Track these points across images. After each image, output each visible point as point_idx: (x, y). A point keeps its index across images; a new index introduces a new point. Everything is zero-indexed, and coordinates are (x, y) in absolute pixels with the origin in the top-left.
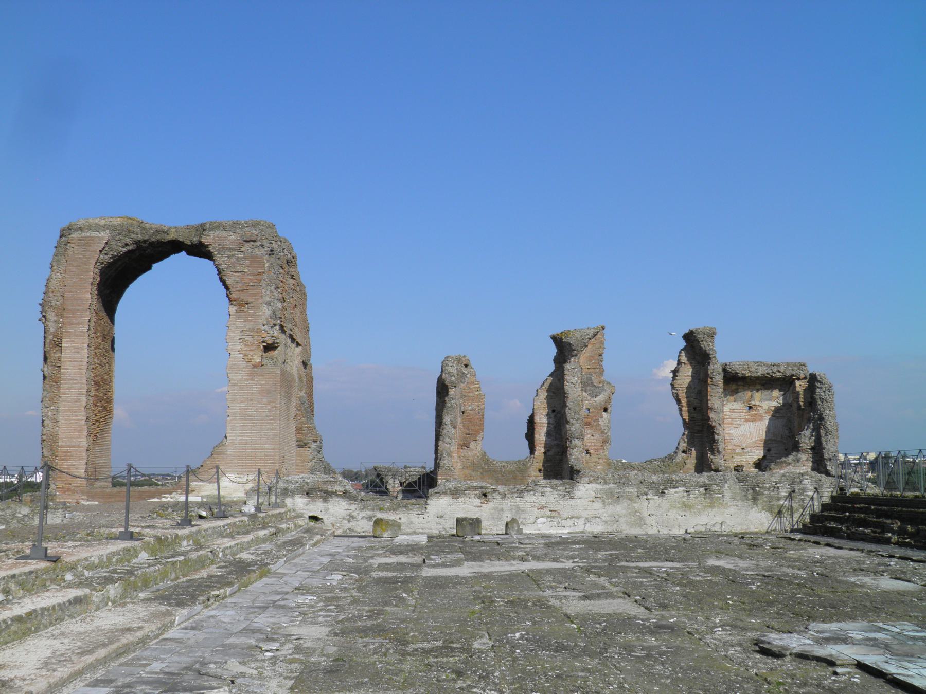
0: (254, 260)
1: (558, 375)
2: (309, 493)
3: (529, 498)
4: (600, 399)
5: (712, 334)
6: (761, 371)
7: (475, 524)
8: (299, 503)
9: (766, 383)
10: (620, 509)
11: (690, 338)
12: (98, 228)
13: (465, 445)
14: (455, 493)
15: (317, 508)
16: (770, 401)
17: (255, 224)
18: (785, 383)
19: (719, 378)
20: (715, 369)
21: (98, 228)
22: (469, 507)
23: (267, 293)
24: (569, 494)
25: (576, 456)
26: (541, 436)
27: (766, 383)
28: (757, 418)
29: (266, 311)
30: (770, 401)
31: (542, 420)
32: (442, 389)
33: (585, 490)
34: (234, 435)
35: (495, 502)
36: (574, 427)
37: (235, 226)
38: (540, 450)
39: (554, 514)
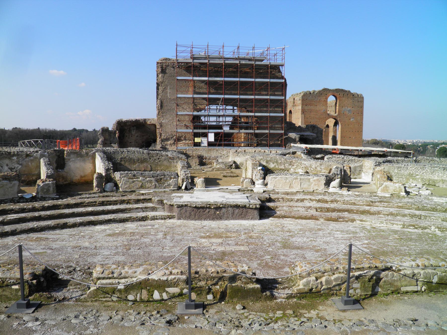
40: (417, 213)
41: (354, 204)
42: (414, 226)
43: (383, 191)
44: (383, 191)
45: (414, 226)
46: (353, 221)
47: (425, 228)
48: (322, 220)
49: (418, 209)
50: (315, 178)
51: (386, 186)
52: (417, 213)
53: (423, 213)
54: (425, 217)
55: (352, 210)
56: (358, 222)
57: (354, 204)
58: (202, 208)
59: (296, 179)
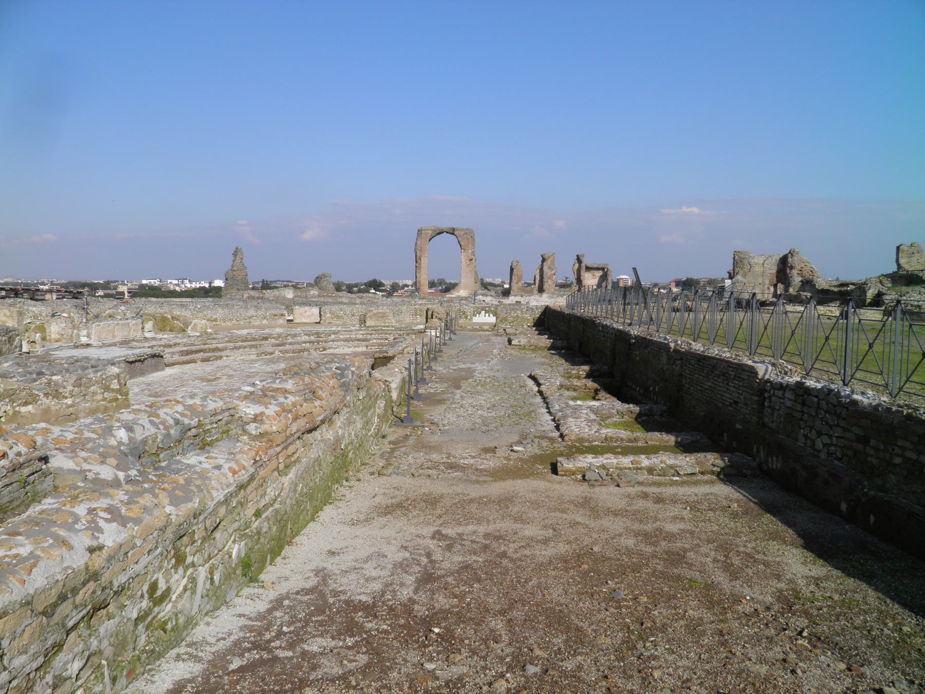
0: (468, 239)
1: (542, 265)
2: (483, 295)
3: (532, 297)
4: (553, 272)
5: (583, 256)
6: (596, 266)
7: (520, 302)
8: (480, 297)
9: (597, 269)
10: (552, 300)
11: (577, 256)
12: (428, 230)
13: (517, 283)
14: (515, 296)
15: (484, 298)
16: (600, 273)
17: (467, 229)
18: (603, 269)
19: (584, 268)
20: (583, 265)
21: (428, 230)
22: (518, 299)
23: (470, 247)
24: (541, 296)
25: (546, 286)
26: (537, 281)
27: (597, 269)
28: (595, 278)
29: (470, 251)
30: (600, 273)
31: (538, 277)
32: (512, 270)
33: (545, 295)
34: (464, 281)
35: (524, 298)
36: (545, 279)
37: (462, 230)
38: (537, 285)
39: (537, 301)
40: (254, 343)
41: (193, 345)
42: (263, 353)
43: (193, 330)
44: (193, 330)
45: (263, 353)
46: (221, 357)
47: (271, 354)
48: (199, 363)
49: (243, 341)
50: (134, 322)
51: (195, 325)
52: (254, 343)
53: (257, 343)
54: (260, 345)
55: (205, 349)
56: (225, 358)
57: (193, 345)
58: (136, 361)
59: (118, 324)
